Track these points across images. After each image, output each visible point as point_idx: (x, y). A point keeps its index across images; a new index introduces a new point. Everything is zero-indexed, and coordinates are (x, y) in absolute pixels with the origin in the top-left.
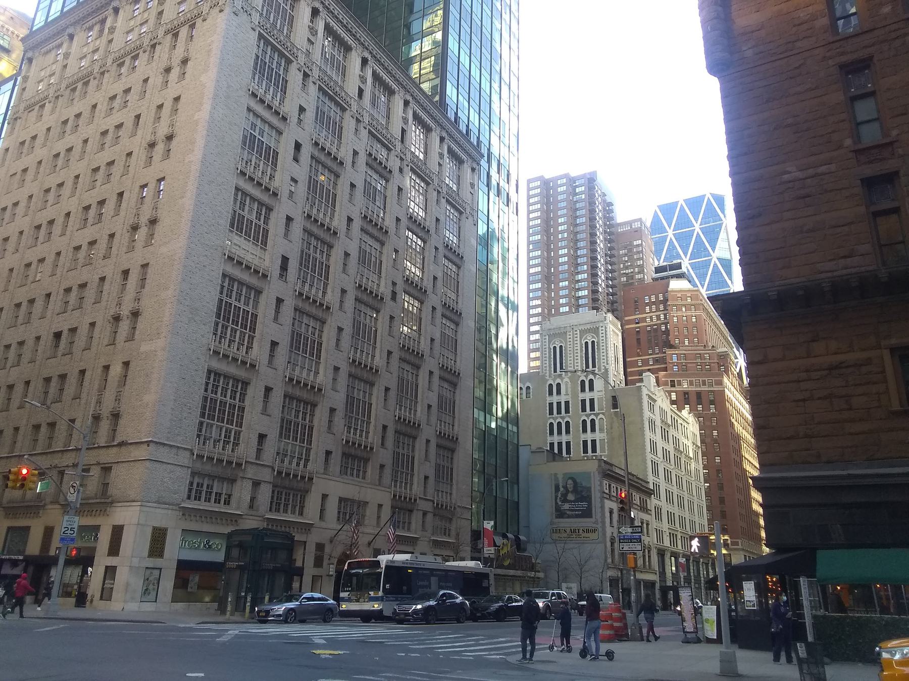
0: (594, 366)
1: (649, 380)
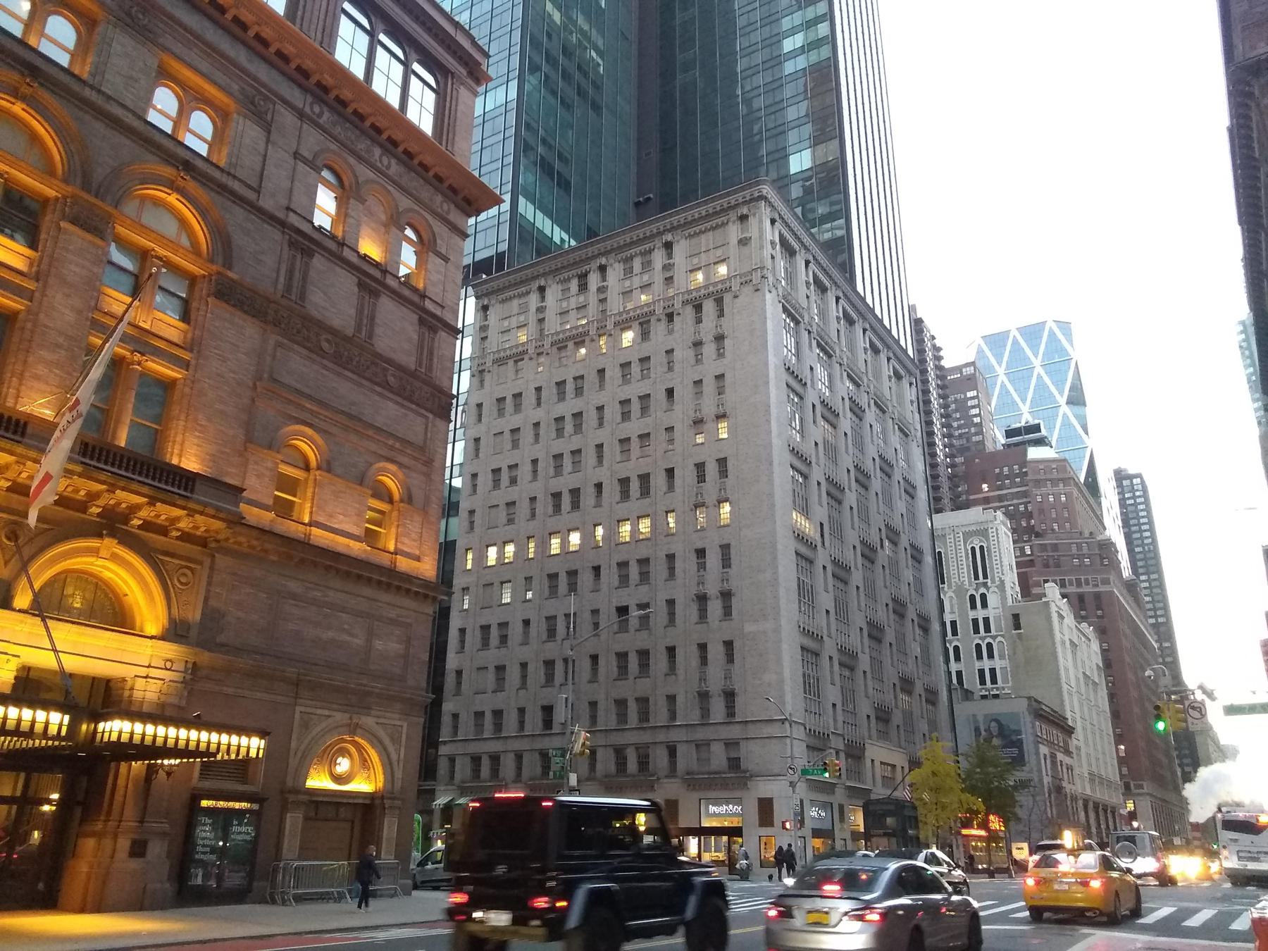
0: (985, 577)
1: (1053, 592)
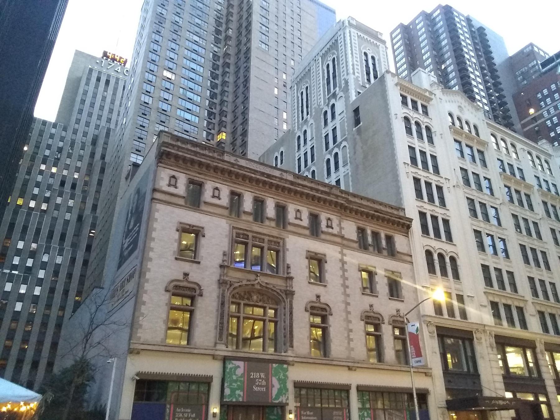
0: (335, 86)
